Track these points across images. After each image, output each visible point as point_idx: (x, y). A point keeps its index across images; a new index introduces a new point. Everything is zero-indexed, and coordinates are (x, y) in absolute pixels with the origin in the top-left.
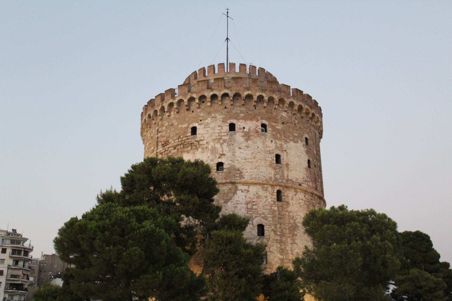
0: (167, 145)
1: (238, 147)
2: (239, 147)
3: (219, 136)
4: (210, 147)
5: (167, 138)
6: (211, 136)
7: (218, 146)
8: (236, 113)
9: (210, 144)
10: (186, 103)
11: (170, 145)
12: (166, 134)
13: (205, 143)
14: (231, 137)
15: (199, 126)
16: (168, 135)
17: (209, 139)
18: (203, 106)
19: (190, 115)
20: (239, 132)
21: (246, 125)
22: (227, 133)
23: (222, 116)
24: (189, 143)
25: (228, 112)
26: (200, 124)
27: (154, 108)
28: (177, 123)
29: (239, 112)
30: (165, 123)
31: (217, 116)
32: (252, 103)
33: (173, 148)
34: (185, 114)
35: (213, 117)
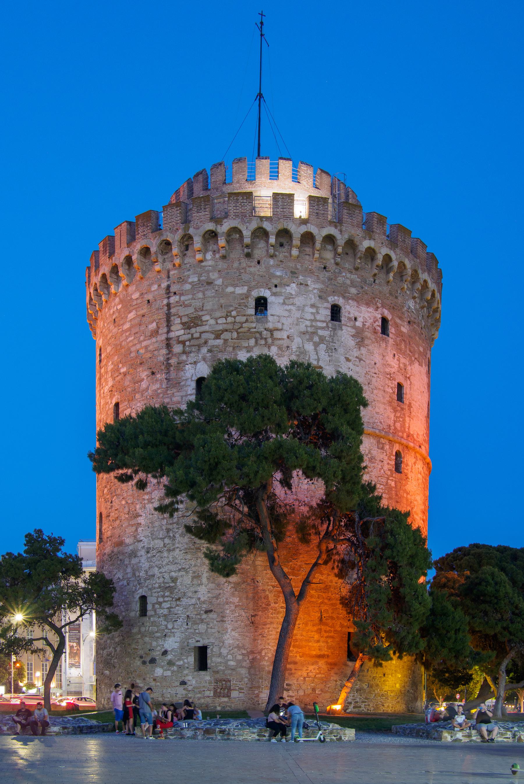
0: (198, 326)
1: (345, 357)
2: (347, 356)
3: (312, 326)
4: (294, 347)
6: (297, 325)
7: (309, 347)
8: (344, 283)
9: (295, 341)
10: (247, 240)
11: (206, 328)
12: (193, 301)
13: (285, 337)
14: (334, 334)
16: (198, 304)
17: (292, 330)
18: (282, 254)
19: (252, 269)
20: (348, 326)
21: (360, 314)
22: (327, 324)
25: (330, 279)
26: (274, 294)
27: (162, 235)
28: (221, 280)
29: (348, 282)
30: (189, 276)
31: (309, 283)
32: (372, 268)
33: (213, 336)
34: (240, 263)
35: (301, 284)
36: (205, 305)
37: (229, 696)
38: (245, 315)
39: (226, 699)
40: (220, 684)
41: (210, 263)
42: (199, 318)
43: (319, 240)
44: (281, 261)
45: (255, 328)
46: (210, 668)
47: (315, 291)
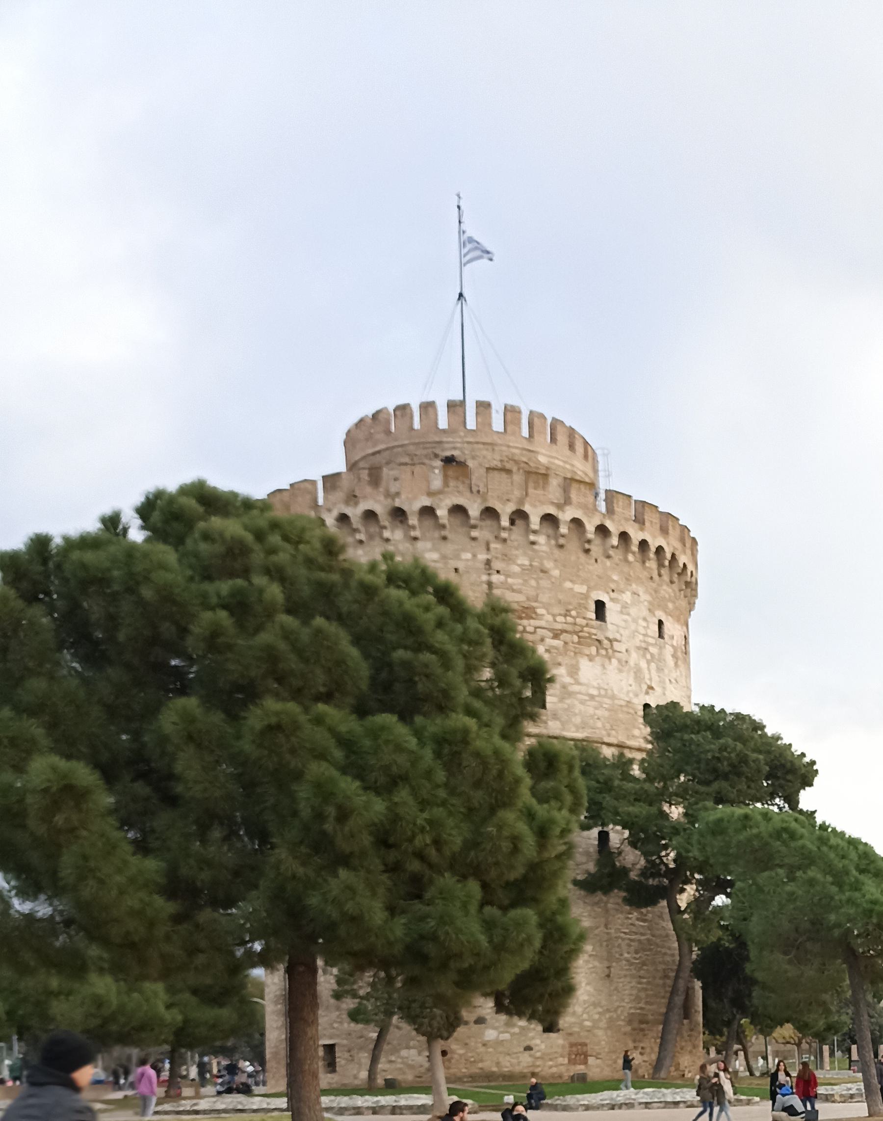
5: (528, 599)
13: (624, 651)
15: (612, 603)
23: (648, 598)
24: (594, 637)
26: (612, 600)
31: (641, 593)
33: (551, 635)
35: (635, 594)
36: (541, 595)
37: (585, 1063)
38: (584, 618)
39: (582, 1067)
40: (574, 1049)
41: (544, 548)
42: (533, 609)
43: (653, 549)
44: (617, 565)
45: (595, 635)
46: (562, 1030)
47: (646, 603)
